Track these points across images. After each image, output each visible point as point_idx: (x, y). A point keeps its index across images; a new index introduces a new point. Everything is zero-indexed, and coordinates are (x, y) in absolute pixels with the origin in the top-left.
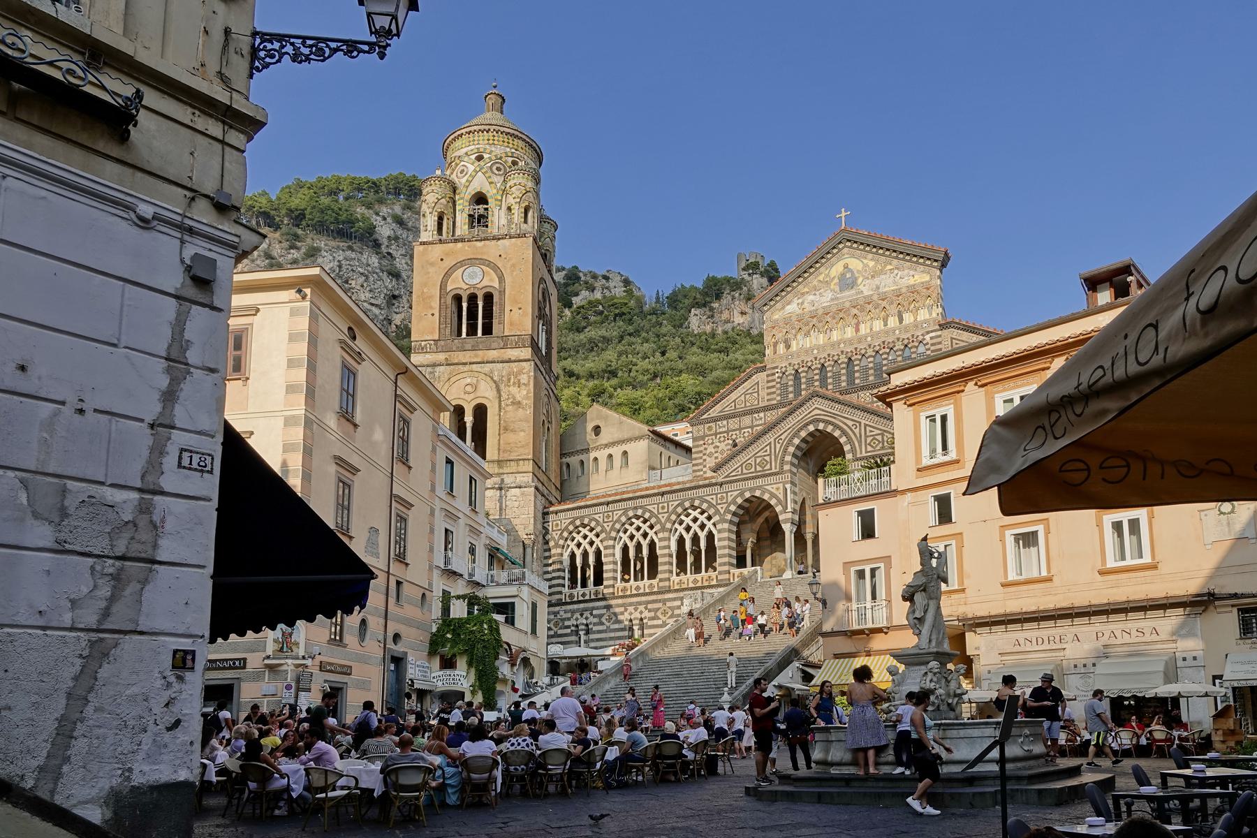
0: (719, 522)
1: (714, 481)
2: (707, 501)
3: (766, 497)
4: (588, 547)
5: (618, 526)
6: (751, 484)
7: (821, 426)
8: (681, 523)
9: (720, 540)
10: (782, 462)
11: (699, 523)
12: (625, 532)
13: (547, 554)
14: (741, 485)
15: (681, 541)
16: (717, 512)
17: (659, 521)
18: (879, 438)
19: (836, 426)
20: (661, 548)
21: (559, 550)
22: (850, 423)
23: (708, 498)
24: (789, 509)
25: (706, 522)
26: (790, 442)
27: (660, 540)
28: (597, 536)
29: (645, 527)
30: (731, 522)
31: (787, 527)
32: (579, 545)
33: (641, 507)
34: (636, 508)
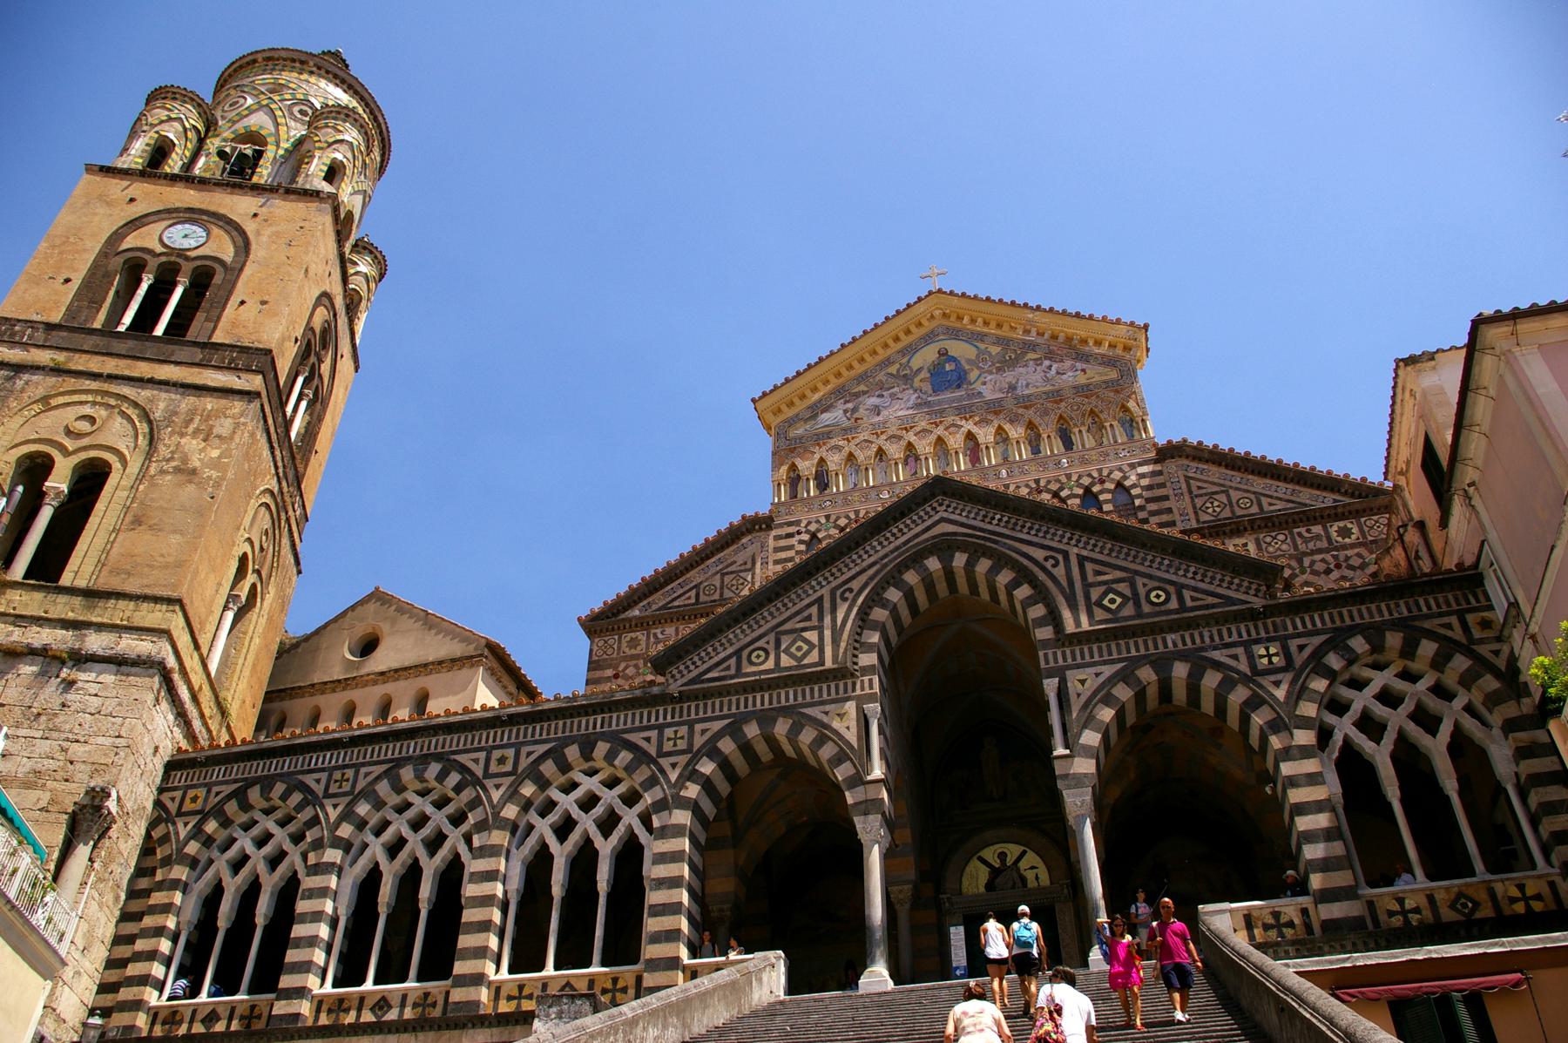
0: (661, 806)
1: (655, 690)
5: (363, 809)
6: (761, 701)
8: (548, 807)
9: (662, 858)
10: (858, 645)
11: (599, 810)
14: (736, 705)
15: (540, 863)
18: (1124, 588)
22: (1039, 554)
23: (635, 738)
25: (621, 809)
28: (297, 838)
29: (439, 819)
30: (695, 808)
33: (438, 757)
34: (424, 760)
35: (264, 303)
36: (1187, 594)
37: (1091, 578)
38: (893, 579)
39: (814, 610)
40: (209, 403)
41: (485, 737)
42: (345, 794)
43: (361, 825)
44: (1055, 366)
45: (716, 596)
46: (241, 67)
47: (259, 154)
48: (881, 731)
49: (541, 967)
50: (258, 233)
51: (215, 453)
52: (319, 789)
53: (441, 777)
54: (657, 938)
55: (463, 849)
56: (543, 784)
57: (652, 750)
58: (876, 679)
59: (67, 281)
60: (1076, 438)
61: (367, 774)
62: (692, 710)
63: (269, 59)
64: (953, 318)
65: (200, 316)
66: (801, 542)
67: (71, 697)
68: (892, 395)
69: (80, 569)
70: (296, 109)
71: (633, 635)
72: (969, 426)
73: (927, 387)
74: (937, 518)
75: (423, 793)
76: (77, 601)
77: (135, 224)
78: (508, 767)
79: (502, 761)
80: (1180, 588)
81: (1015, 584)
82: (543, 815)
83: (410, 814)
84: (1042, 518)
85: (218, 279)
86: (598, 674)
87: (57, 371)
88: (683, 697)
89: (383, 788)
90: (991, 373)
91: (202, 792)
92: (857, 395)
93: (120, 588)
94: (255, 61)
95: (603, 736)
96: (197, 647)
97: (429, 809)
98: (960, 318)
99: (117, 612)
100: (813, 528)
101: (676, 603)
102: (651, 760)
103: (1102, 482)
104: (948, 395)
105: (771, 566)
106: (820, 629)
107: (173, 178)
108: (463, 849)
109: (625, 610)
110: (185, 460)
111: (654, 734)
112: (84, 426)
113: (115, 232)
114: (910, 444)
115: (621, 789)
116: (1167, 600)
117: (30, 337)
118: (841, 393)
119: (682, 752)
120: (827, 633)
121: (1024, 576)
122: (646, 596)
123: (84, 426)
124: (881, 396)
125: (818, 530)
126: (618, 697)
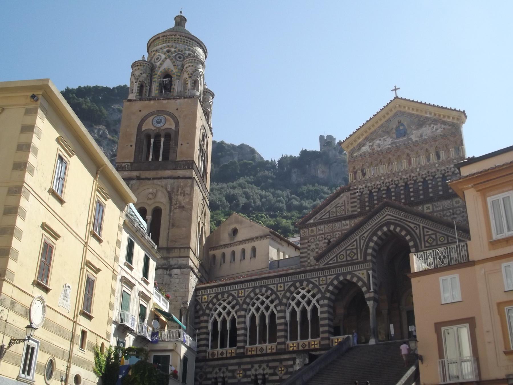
1: (317, 267)
2: (312, 283)
3: (355, 280)
4: (226, 316)
5: (248, 300)
6: (343, 270)
7: (392, 228)
8: (293, 299)
9: (322, 313)
10: (366, 254)
11: (306, 299)
12: (253, 305)
13: (197, 320)
14: (336, 271)
15: (293, 313)
16: (320, 291)
17: (277, 297)
19: (403, 228)
20: (280, 318)
21: (205, 318)
22: (412, 226)
23: (313, 280)
24: (372, 290)
25: (311, 298)
26: (370, 240)
27: (279, 312)
28: (233, 307)
29: (267, 302)
30: (329, 299)
31: (370, 304)
32: (220, 314)
35: (188, 143)
36: (450, 238)
37: (425, 233)
38: (375, 234)
39: (355, 243)
40: (182, 182)
41: (276, 280)
42: (243, 297)
43: (248, 304)
44: (435, 127)
45: (335, 215)
46: (155, 40)
47: (171, 82)
48: (373, 277)
49: (297, 339)
50: (180, 116)
51: (187, 200)
52: (236, 295)
53: (266, 291)
54: (323, 332)
55: (274, 310)
56: (292, 293)
57: (317, 284)
58: (371, 263)
59: (131, 146)
60: (441, 155)
61: (247, 291)
62: (326, 273)
63: (163, 36)
64: (402, 108)
65: (171, 151)
66: (358, 196)
67: (172, 279)
68: (384, 139)
69: (163, 242)
70: (177, 57)
71: (311, 229)
72: (407, 151)
73: (394, 136)
74: (386, 214)
75: (262, 295)
76: (165, 252)
77: (143, 121)
78: (282, 289)
79: (281, 287)
80: (448, 236)
81: (406, 235)
82: (293, 300)
83: (260, 300)
84: (413, 214)
85: (173, 136)
86: (303, 242)
87: (138, 178)
88: (322, 269)
89: (252, 295)
90: (415, 130)
91: (206, 297)
92: (373, 140)
93: (174, 246)
94: (159, 38)
95: (305, 280)
96: (195, 255)
97: (265, 300)
98: (404, 107)
99: (176, 253)
100: (362, 190)
101: (323, 218)
102: (317, 287)
103: (448, 172)
104: (401, 139)
105: (350, 204)
106: (356, 248)
107: (150, 100)
108: (274, 310)
109: (309, 220)
110: (180, 204)
111: (317, 279)
112: (150, 196)
113: (139, 125)
114: (390, 158)
115: (311, 293)
116: (444, 240)
117: (127, 168)
118: (367, 139)
119: (324, 284)
120: (359, 250)
121: (408, 233)
122: (314, 216)
123: (150, 196)
124: (380, 140)
125: (363, 191)
126: (308, 268)
